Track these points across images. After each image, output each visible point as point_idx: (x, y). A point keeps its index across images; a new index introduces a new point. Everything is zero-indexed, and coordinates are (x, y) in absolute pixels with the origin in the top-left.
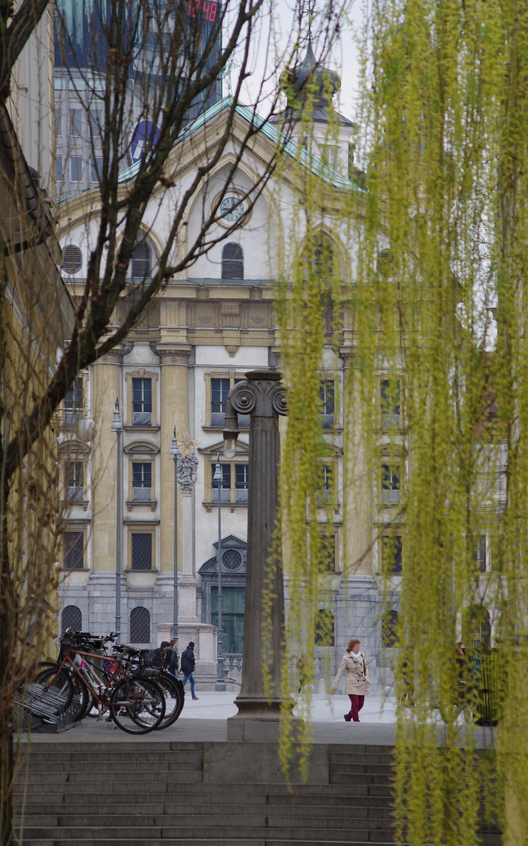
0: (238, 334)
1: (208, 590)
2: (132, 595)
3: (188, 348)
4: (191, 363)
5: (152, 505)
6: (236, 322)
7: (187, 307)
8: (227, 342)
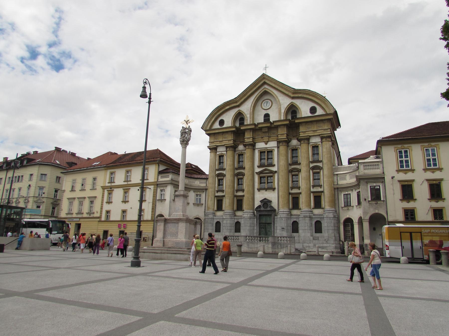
0: (268, 138)
1: (258, 215)
2: (235, 218)
5: (243, 191)
6: (267, 134)
8: (264, 140)
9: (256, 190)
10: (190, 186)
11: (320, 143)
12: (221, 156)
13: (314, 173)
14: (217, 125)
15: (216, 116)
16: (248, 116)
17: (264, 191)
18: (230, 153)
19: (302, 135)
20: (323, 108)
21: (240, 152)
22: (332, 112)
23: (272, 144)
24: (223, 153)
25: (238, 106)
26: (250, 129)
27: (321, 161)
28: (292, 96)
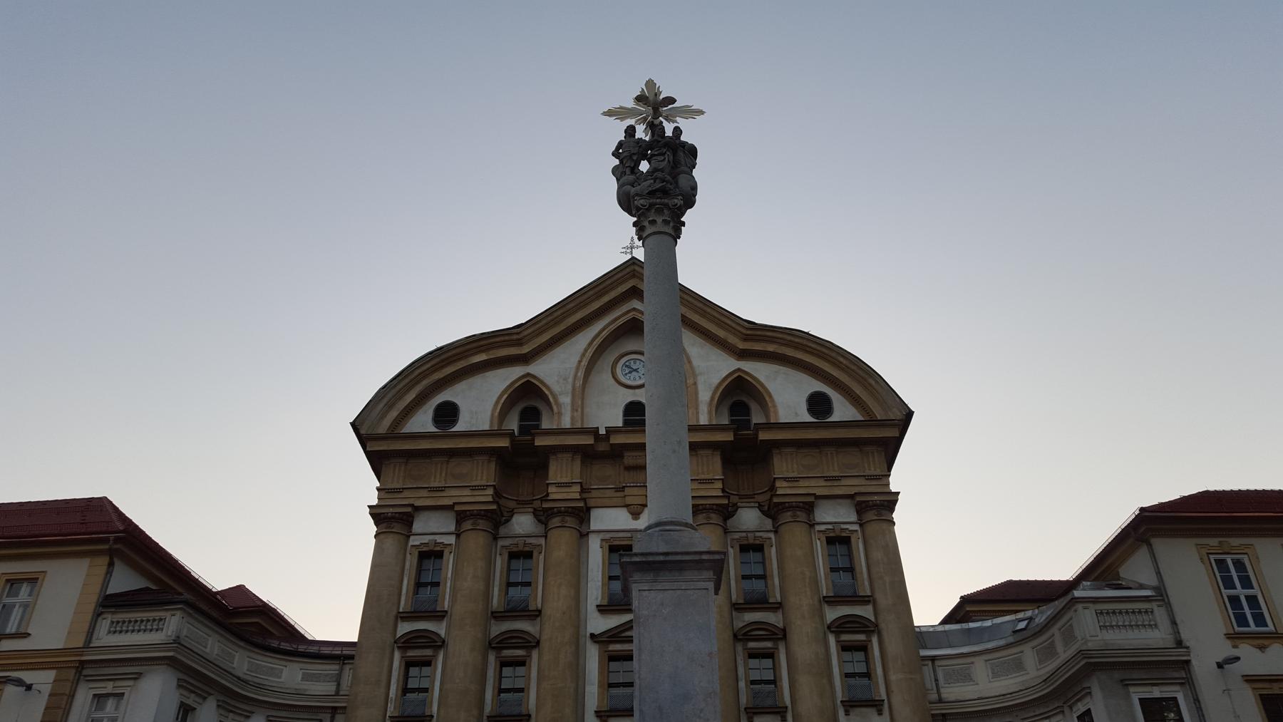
3: (581, 504)
4: (584, 530)
7: (583, 462)
8: (629, 500)
10: (259, 687)
11: (856, 527)
12: (431, 555)
13: (845, 648)
14: (423, 421)
15: (425, 383)
16: (566, 400)
18: (476, 541)
19: (783, 488)
20: (855, 401)
21: (521, 541)
22: (897, 415)
24: (440, 539)
25: (525, 359)
26: (575, 449)
27: (865, 601)
28: (741, 345)
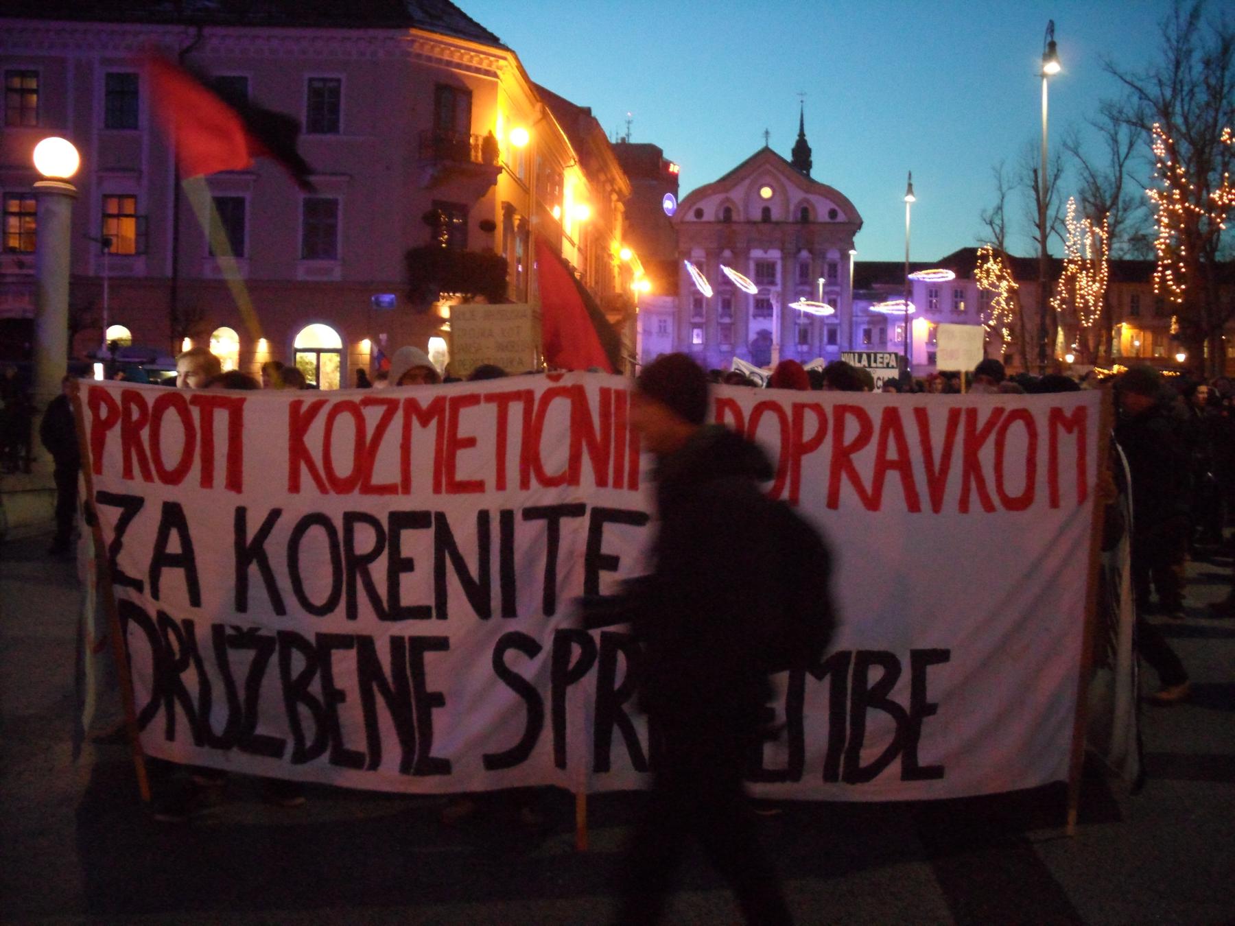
9: (751, 318)
17: (761, 319)
23: (774, 254)
